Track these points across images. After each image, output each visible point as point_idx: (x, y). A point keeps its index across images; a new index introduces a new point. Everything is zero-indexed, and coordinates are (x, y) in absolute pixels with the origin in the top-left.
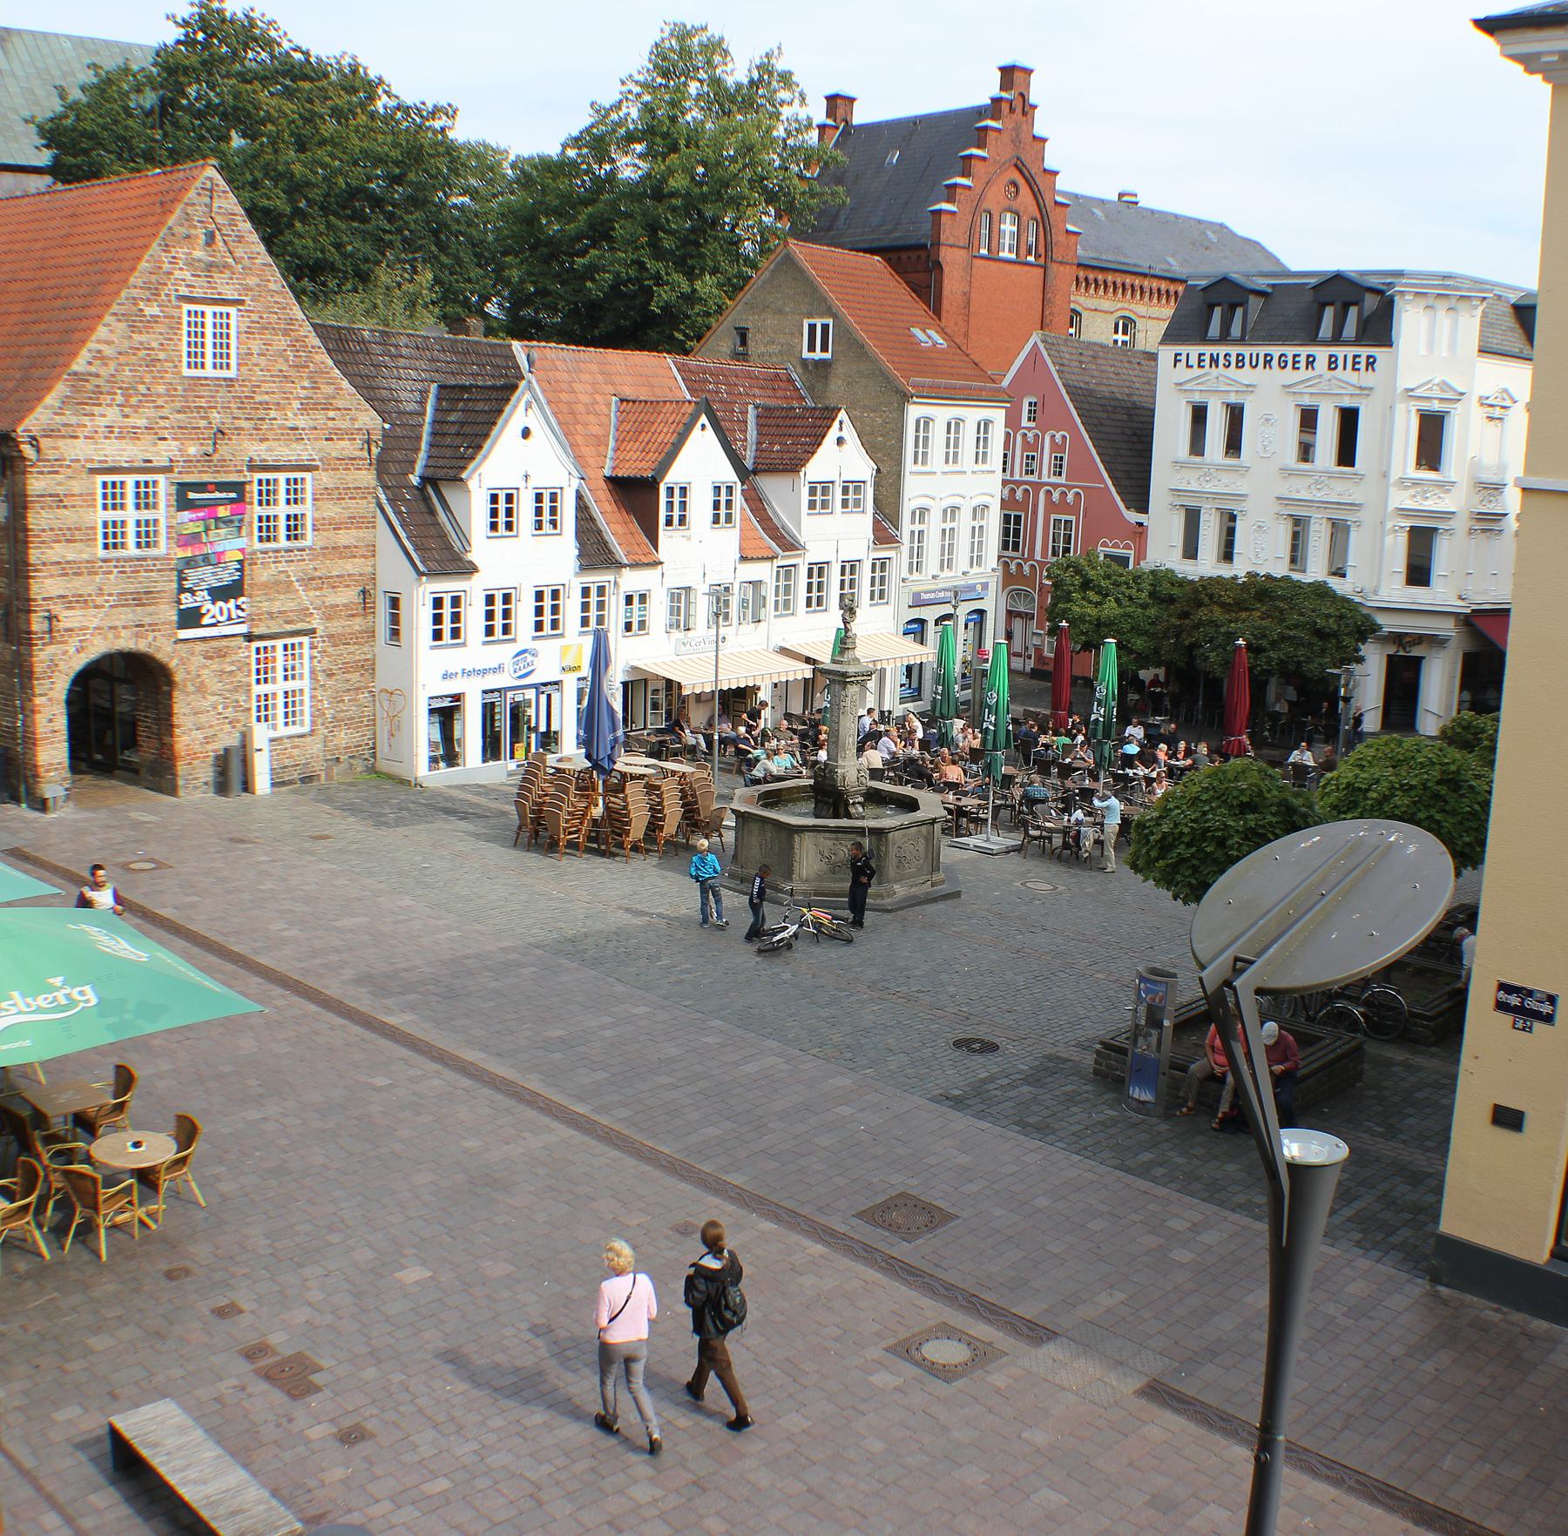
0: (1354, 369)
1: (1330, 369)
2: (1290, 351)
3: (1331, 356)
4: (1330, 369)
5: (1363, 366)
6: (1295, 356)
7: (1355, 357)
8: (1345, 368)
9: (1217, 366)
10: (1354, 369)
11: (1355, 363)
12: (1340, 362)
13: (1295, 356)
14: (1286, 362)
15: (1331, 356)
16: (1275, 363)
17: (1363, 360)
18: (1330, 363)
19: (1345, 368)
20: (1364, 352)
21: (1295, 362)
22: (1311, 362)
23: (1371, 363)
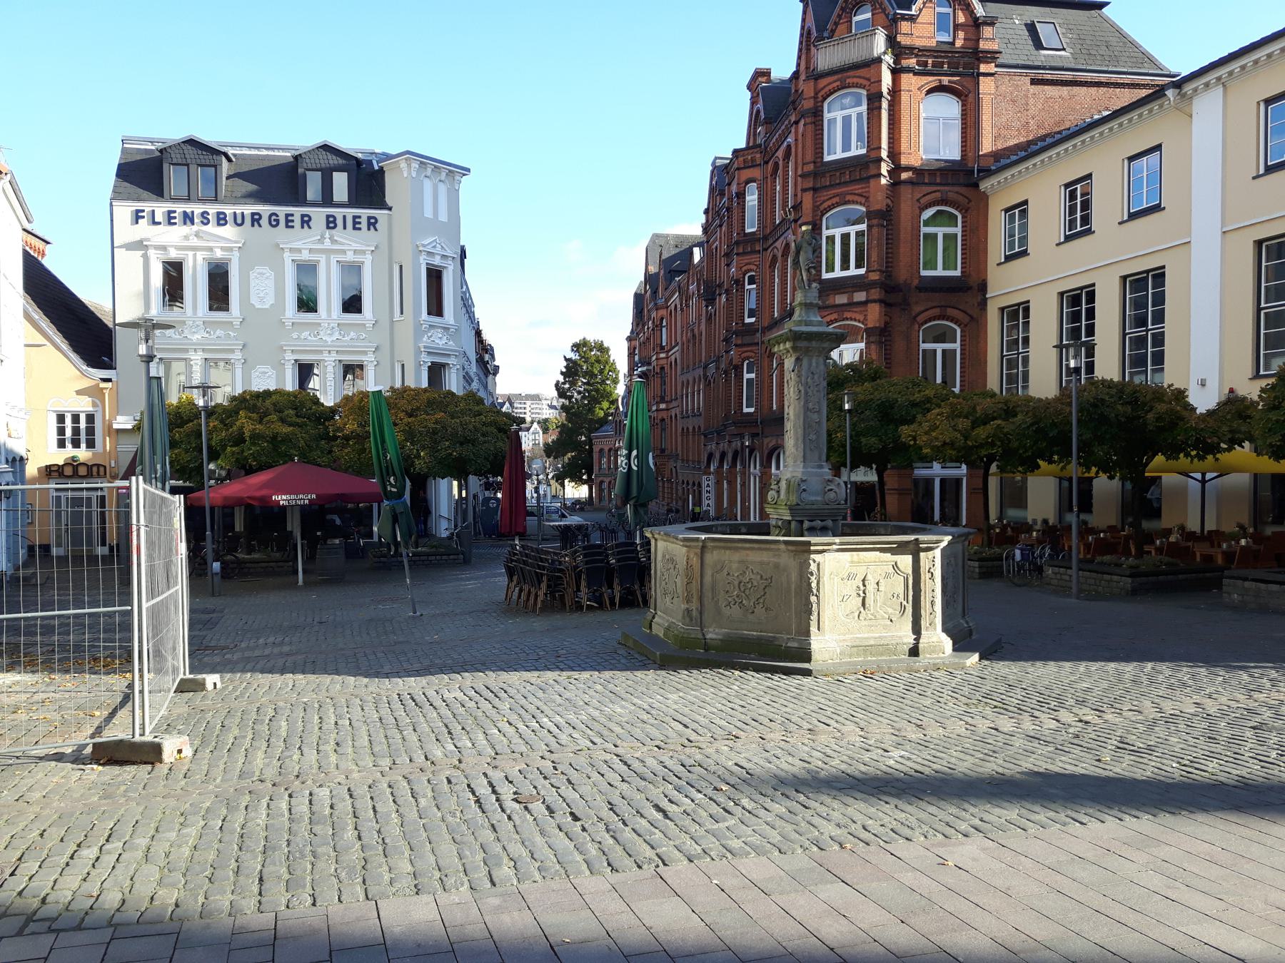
0: (355, 228)
1: (328, 227)
2: (282, 210)
3: (328, 217)
4: (328, 227)
5: (364, 225)
6: (287, 215)
7: (355, 217)
8: (345, 228)
9: (193, 224)
10: (355, 228)
11: (355, 223)
12: (340, 222)
13: (287, 215)
14: (278, 221)
15: (328, 217)
16: (264, 221)
17: (364, 221)
18: (328, 222)
19: (345, 228)
20: (365, 213)
21: (287, 221)
22: (306, 221)
23: (372, 223)
